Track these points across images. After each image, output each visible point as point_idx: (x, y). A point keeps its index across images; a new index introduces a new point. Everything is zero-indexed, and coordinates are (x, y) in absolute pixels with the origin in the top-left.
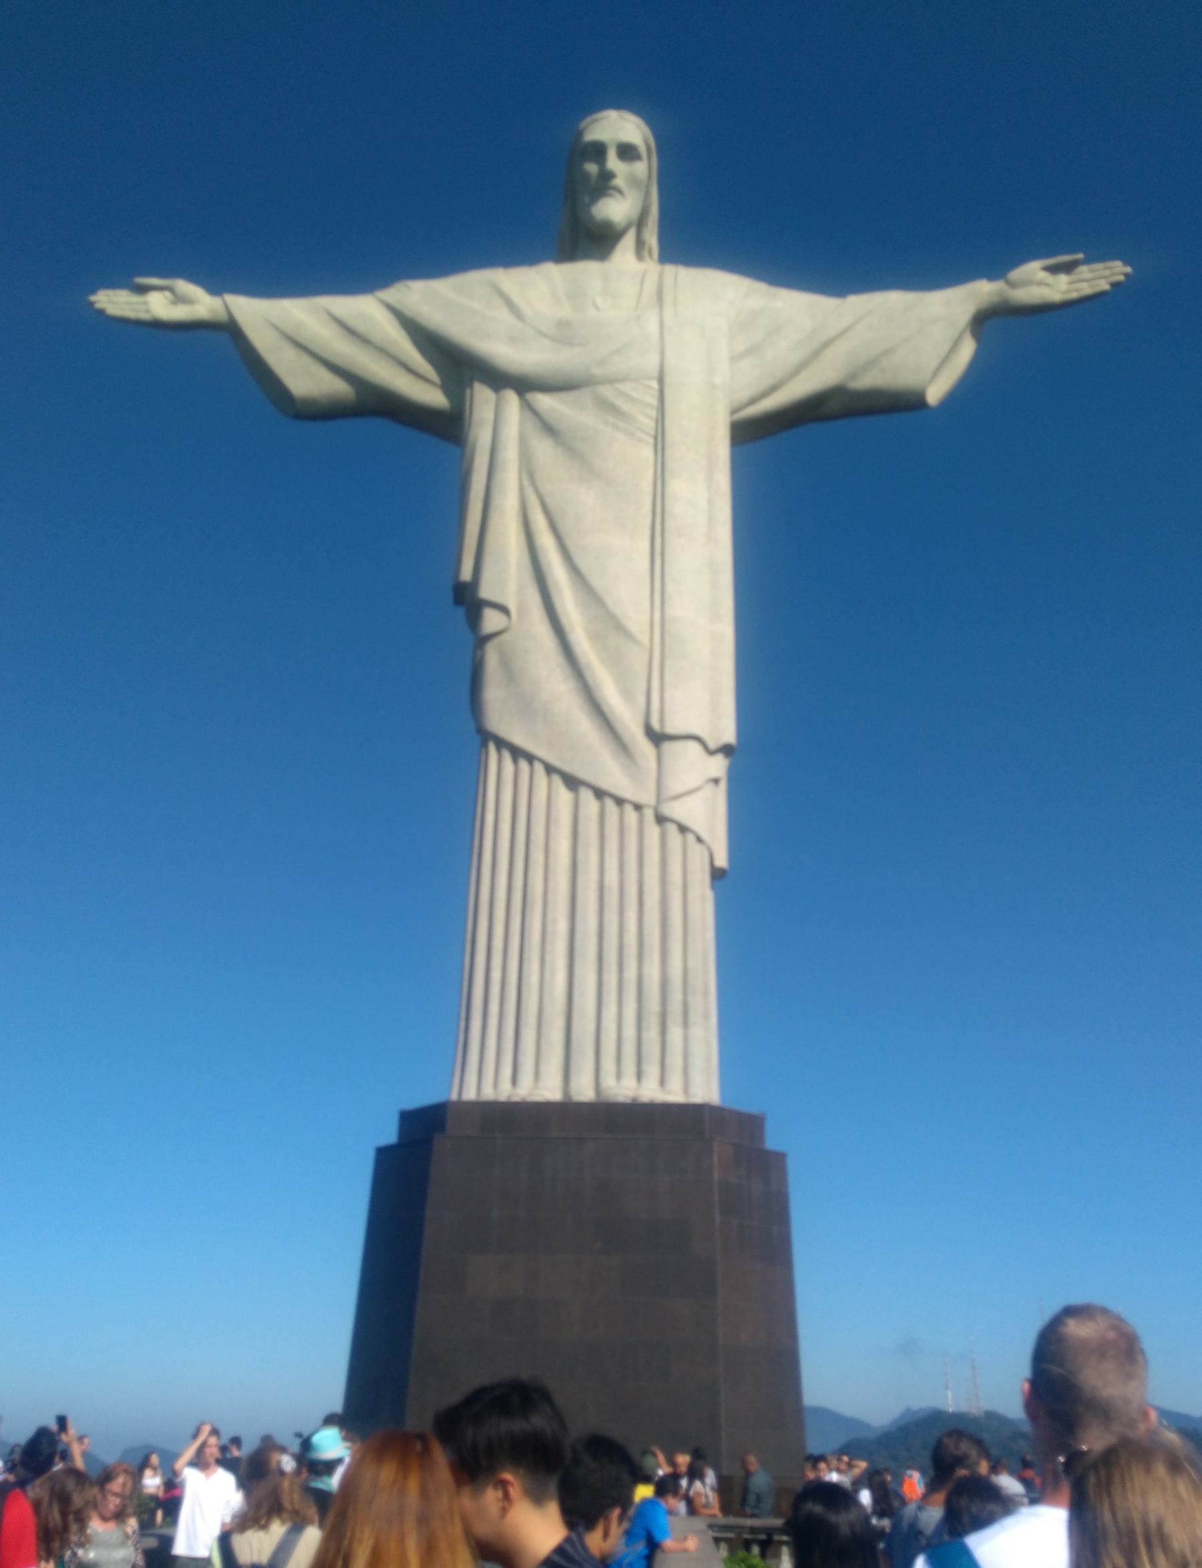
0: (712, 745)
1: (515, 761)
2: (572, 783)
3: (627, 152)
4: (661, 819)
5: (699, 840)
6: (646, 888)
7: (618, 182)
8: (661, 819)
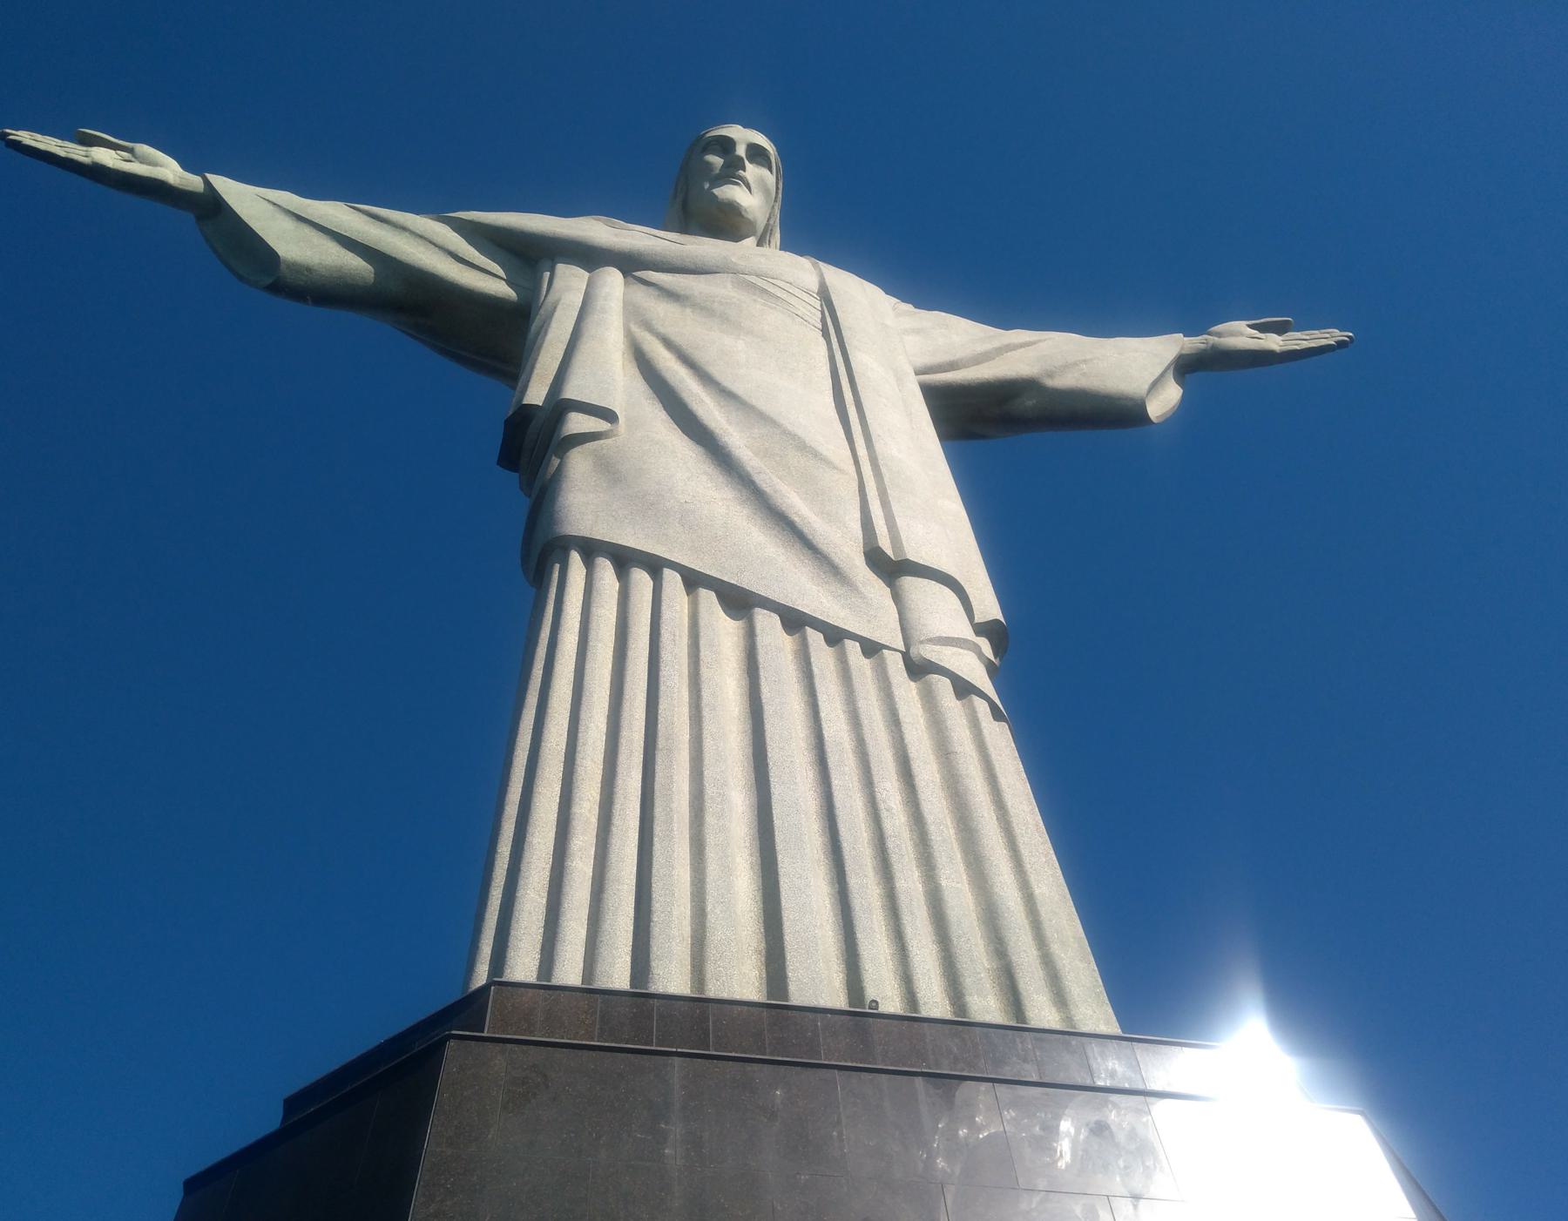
0: (978, 619)
2: (739, 602)
3: (756, 153)
4: (918, 669)
6: (913, 752)
8: (918, 669)
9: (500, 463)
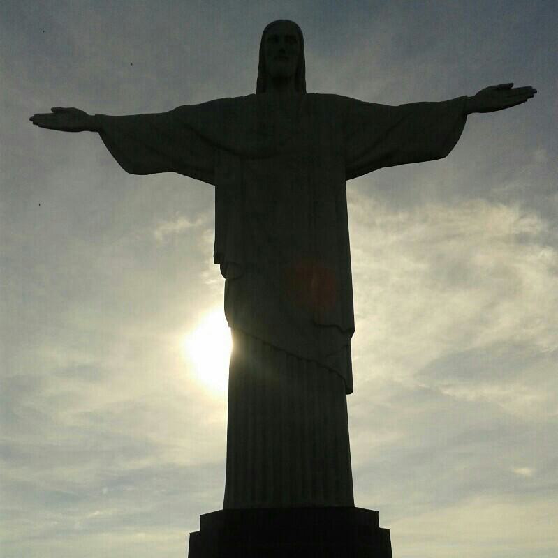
9: (215, 263)
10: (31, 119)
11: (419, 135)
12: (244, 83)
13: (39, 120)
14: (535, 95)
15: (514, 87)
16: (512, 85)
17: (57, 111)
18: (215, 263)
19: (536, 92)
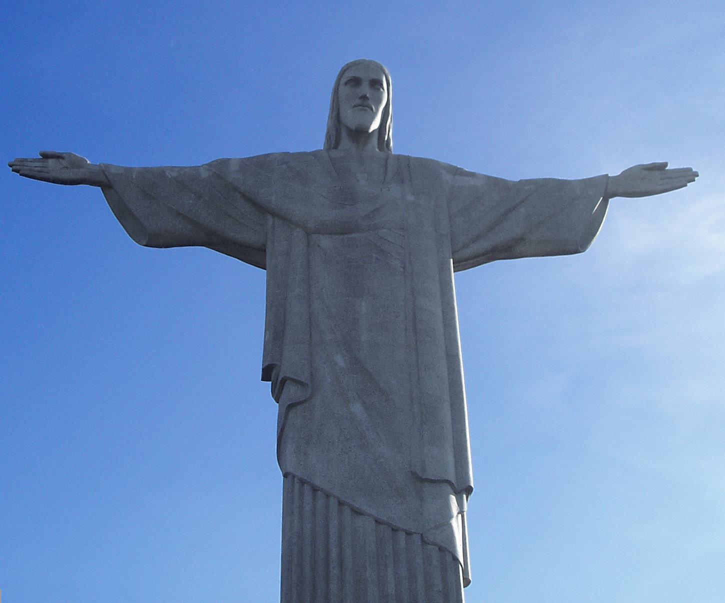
1: (314, 498)
4: (424, 542)
5: (455, 559)
7: (370, 102)
8: (424, 542)
9: (262, 380)
10: (11, 166)
11: (552, 220)
12: (309, 134)
13: (20, 168)
14: (696, 178)
15: (667, 168)
16: (666, 165)
17: (46, 156)
18: (266, 377)
19: (698, 176)
